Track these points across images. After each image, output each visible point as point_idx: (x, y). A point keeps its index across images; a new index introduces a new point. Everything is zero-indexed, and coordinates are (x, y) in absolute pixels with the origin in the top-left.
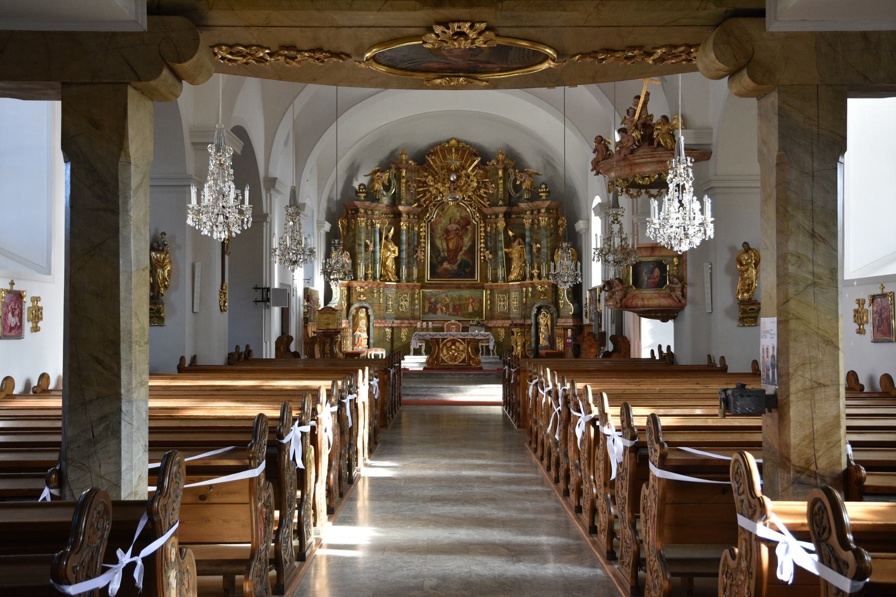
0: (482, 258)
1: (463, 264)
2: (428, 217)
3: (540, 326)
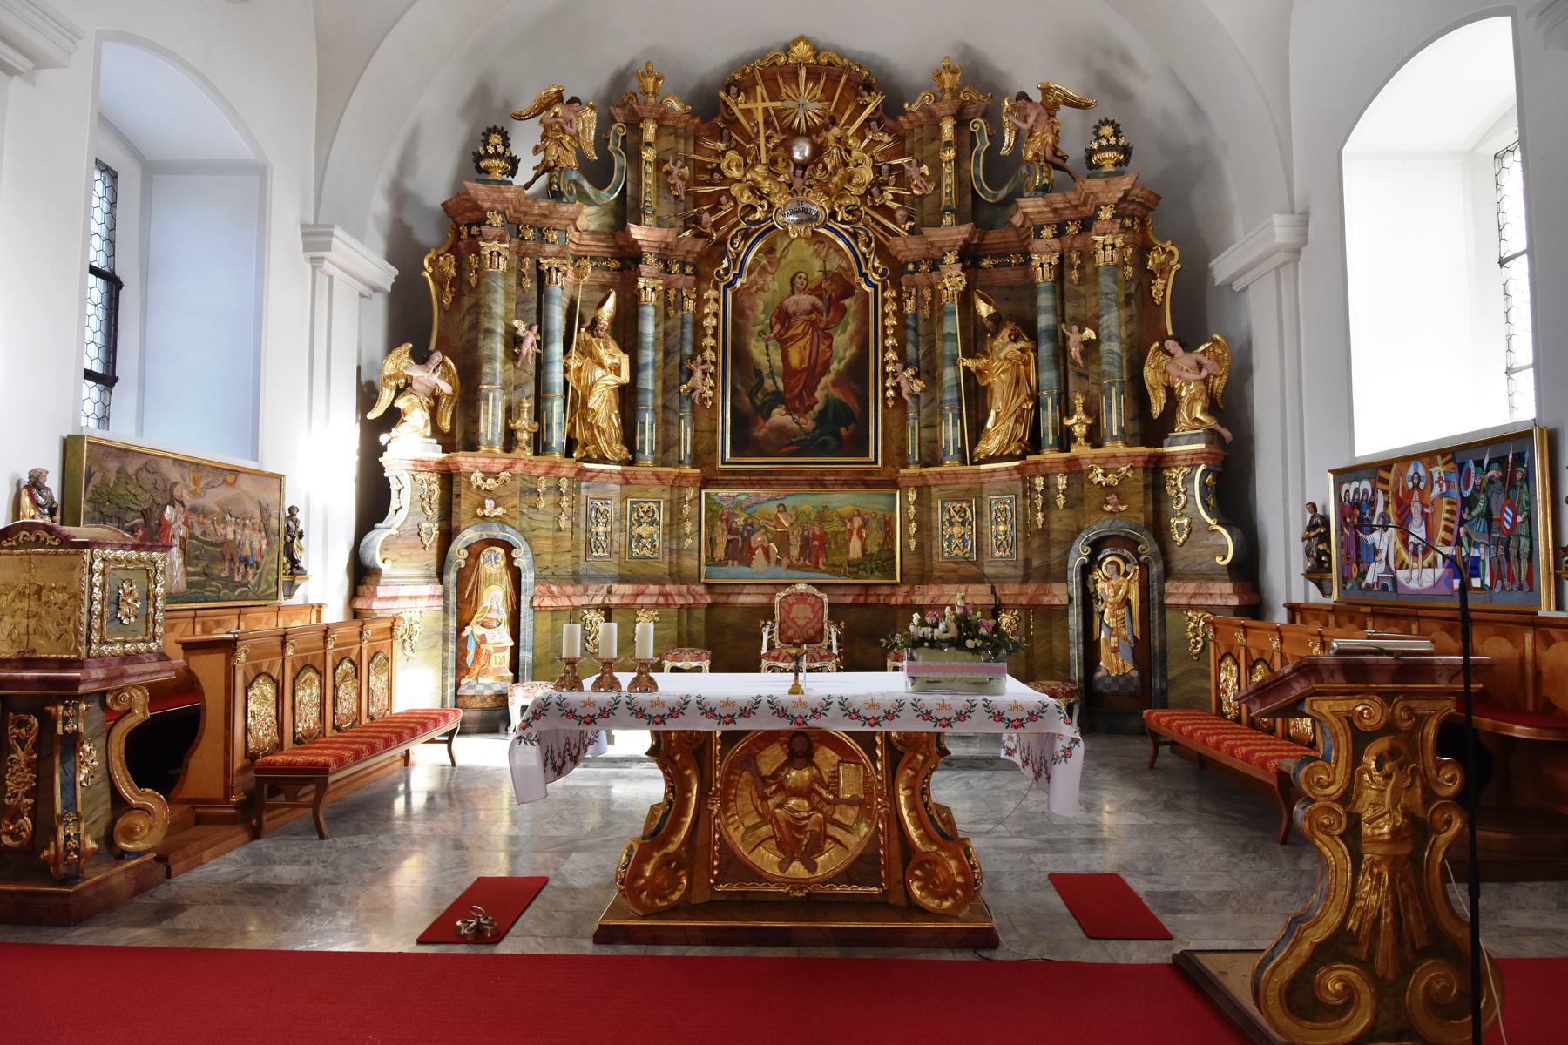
0: (890, 393)
1: (831, 414)
2: (727, 271)
3: (1099, 607)
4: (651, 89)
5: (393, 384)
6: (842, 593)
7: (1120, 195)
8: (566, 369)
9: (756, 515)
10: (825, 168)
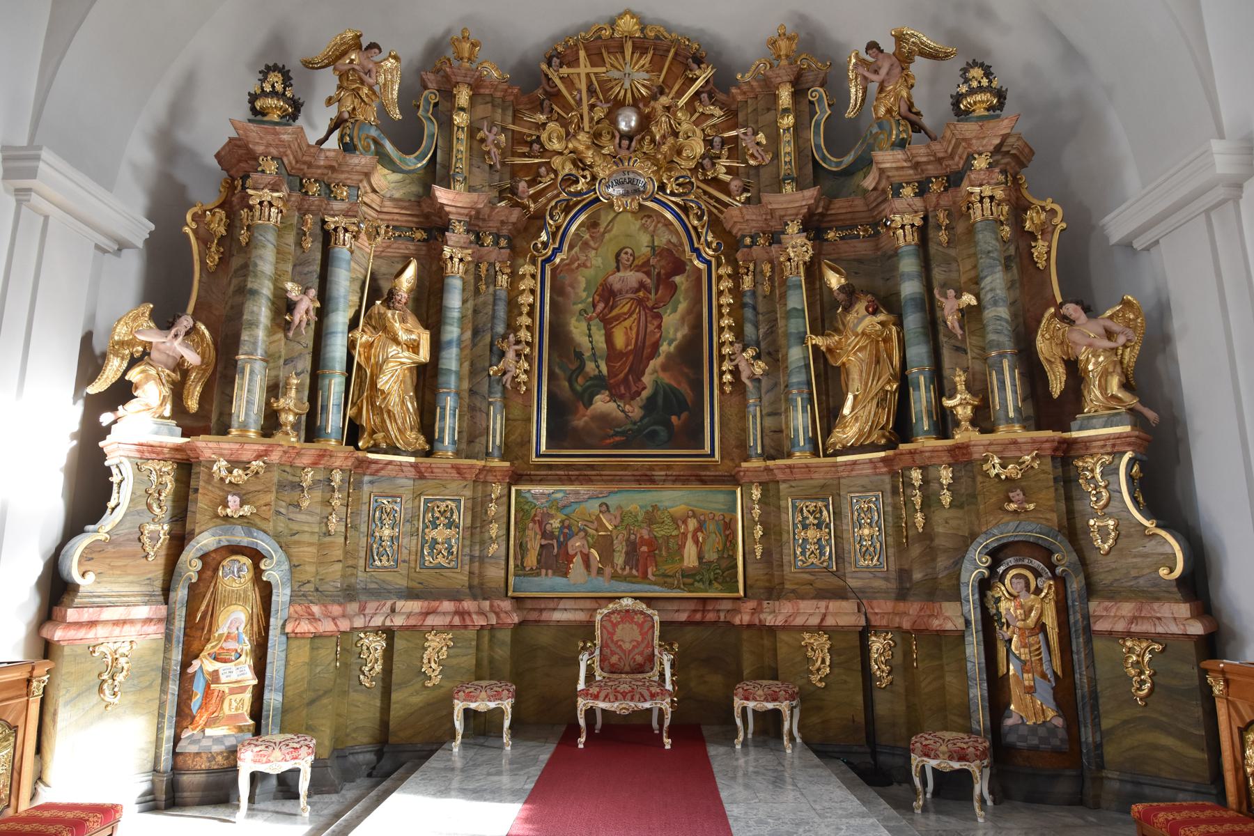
0: (728, 377)
1: (660, 401)
2: (545, 245)
3: (1005, 633)
4: (466, 55)
5: (127, 352)
6: (676, 608)
7: (997, 141)
8: (351, 345)
9: (574, 516)
10: (653, 141)
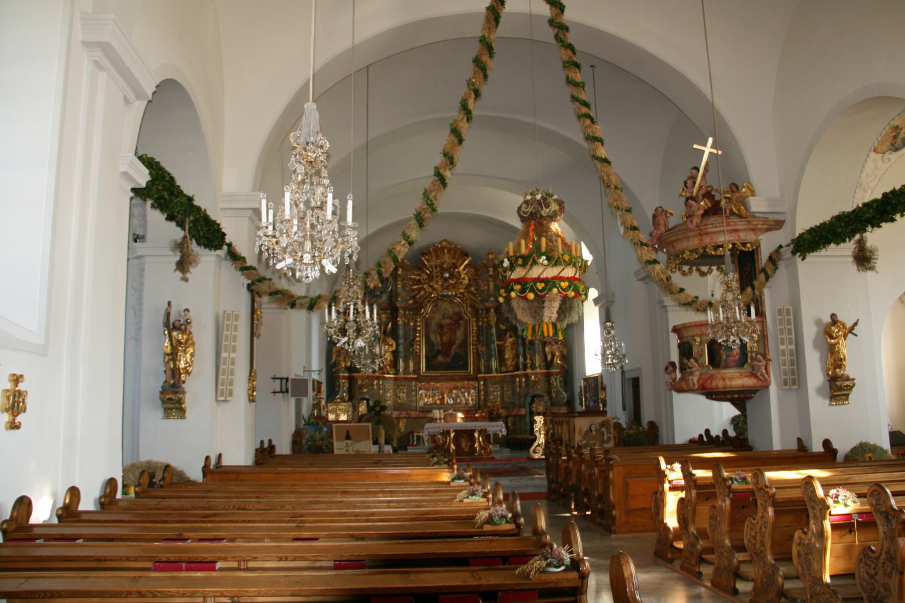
2: (423, 313)
